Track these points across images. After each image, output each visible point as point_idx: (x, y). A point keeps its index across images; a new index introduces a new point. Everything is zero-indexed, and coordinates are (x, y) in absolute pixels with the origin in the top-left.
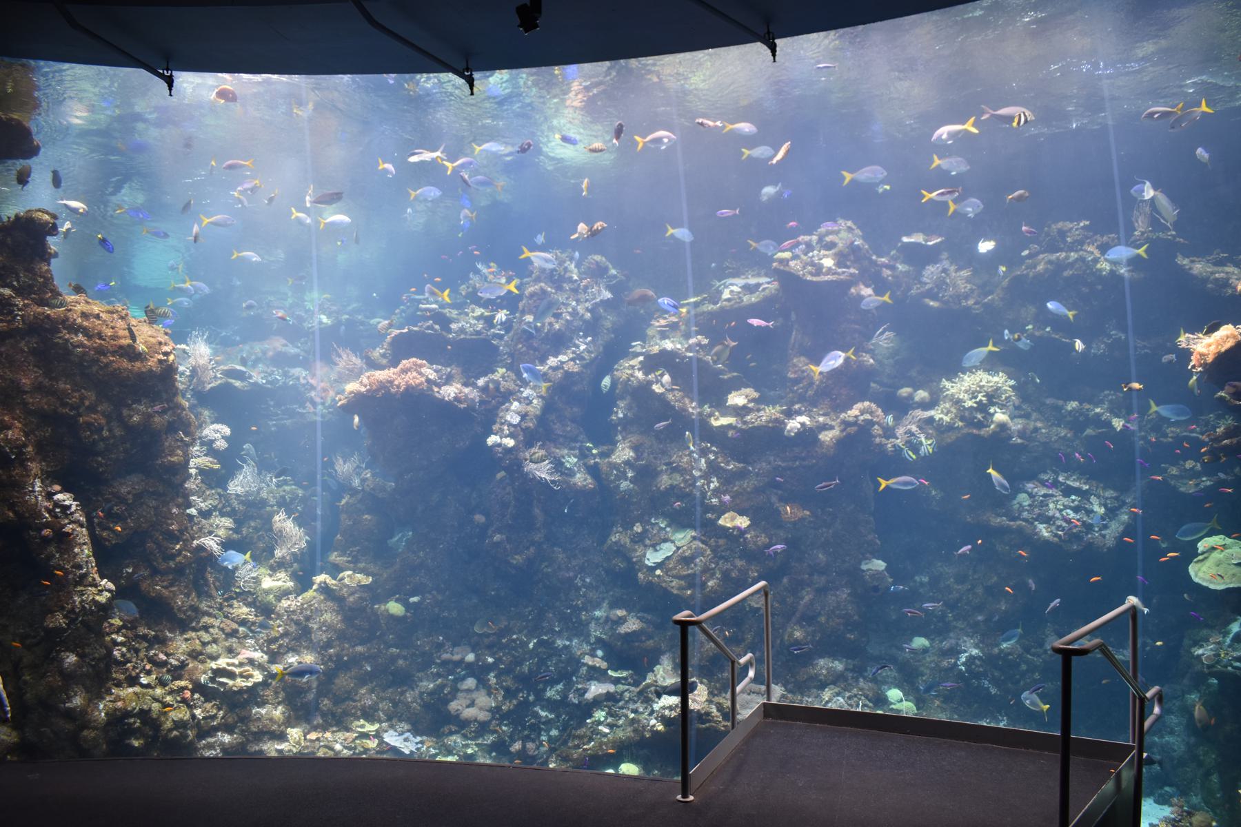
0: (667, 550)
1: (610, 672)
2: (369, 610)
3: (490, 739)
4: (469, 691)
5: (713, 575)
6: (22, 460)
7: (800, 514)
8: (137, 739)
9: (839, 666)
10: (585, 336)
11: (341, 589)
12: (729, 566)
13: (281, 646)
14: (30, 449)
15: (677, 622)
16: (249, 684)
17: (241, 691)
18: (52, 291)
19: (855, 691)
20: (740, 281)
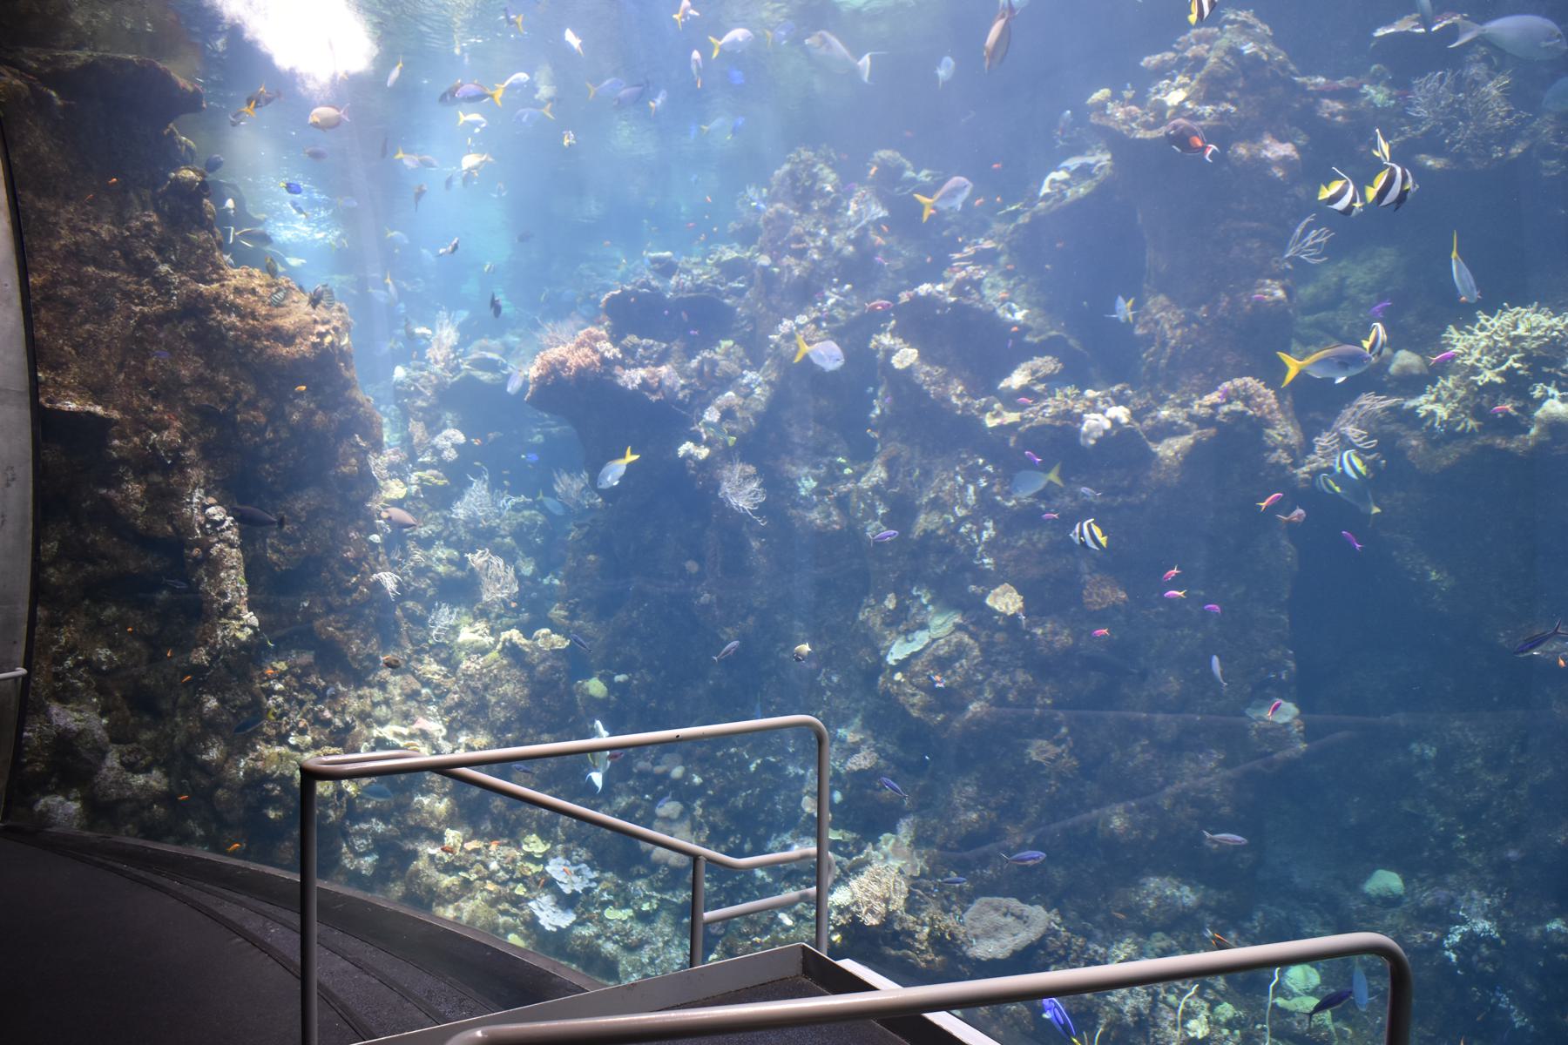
0: (921, 639)
6: (179, 465)
8: (275, 809)
9: (1188, 896)
10: (842, 283)
14: (191, 453)
18: (213, 264)
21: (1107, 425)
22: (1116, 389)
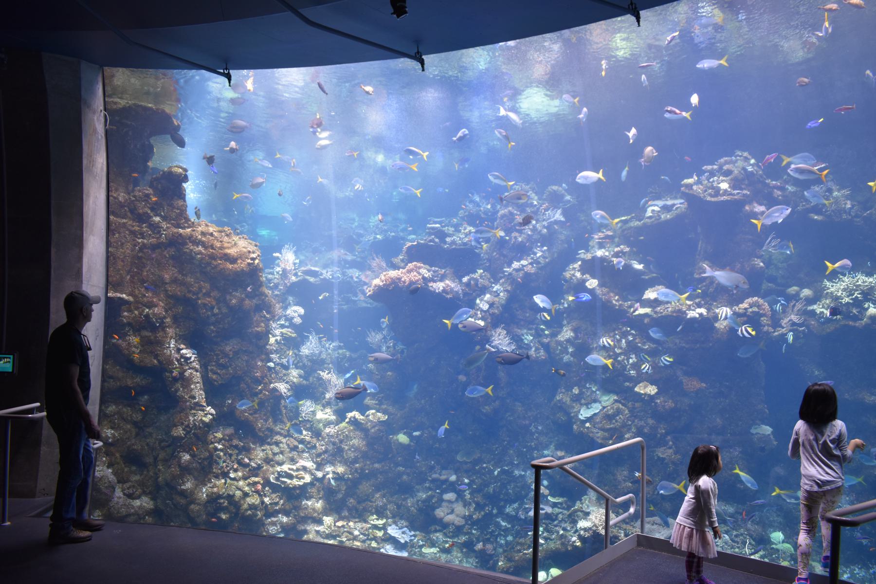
0: (596, 408)
1: (549, 498)
2: (384, 439)
3: (463, 538)
4: (450, 502)
5: (630, 429)
6: (163, 326)
7: (698, 386)
8: (225, 514)
10: (542, 246)
11: (367, 423)
12: (642, 423)
13: (323, 459)
14: (168, 320)
15: (534, 466)
16: (301, 484)
17: (295, 488)
19: (742, 530)
20: (660, 203)
21: (697, 316)
22: (697, 301)
